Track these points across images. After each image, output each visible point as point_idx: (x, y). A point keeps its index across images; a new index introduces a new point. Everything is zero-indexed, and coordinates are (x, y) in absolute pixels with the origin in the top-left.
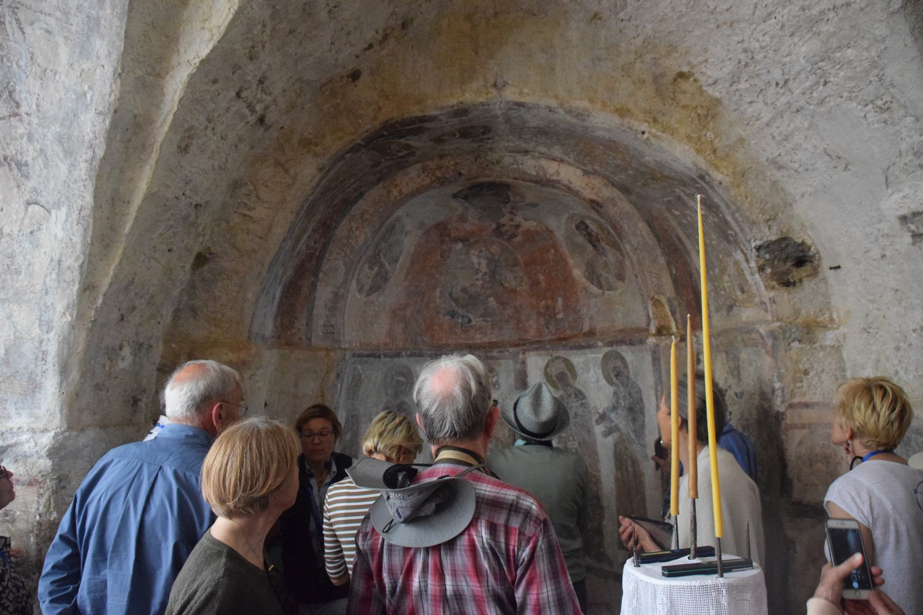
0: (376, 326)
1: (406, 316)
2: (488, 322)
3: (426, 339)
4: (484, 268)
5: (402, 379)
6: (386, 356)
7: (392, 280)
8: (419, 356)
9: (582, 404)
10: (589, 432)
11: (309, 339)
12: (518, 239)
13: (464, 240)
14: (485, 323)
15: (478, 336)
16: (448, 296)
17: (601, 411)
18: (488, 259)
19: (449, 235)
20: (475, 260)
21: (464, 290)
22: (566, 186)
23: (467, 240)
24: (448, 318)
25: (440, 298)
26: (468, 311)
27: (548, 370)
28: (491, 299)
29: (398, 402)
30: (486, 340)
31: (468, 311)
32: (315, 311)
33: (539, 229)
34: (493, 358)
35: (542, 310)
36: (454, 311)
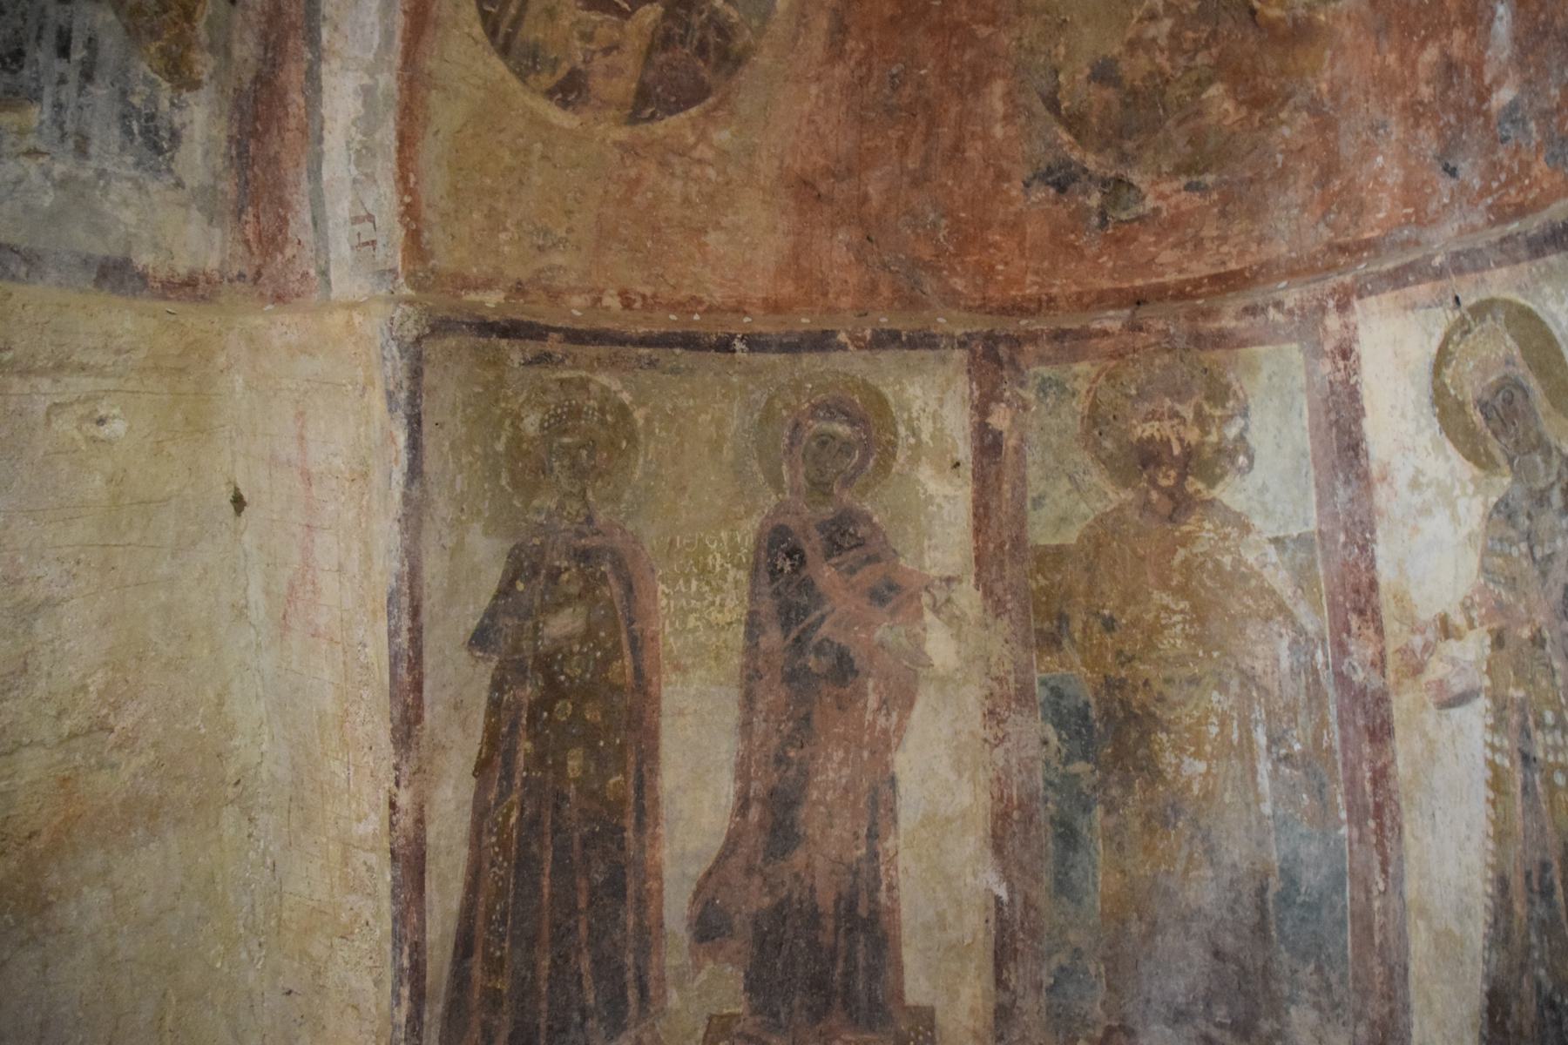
0: (712, 238)
1: (865, 199)
3: (959, 284)
5: (842, 429)
6: (755, 343)
7: (763, 59)
11: (324, 273)
14: (1196, 197)
15: (1167, 256)
16: (1039, 107)
21: (1104, 73)
24: (1042, 193)
25: (1007, 119)
26: (1123, 158)
27: (1448, 372)
28: (1215, 90)
29: (828, 511)
30: (1200, 268)
31: (1123, 158)
32: (326, 174)
34: (1222, 340)
35: (1426, 92)
36: (1068, 164)
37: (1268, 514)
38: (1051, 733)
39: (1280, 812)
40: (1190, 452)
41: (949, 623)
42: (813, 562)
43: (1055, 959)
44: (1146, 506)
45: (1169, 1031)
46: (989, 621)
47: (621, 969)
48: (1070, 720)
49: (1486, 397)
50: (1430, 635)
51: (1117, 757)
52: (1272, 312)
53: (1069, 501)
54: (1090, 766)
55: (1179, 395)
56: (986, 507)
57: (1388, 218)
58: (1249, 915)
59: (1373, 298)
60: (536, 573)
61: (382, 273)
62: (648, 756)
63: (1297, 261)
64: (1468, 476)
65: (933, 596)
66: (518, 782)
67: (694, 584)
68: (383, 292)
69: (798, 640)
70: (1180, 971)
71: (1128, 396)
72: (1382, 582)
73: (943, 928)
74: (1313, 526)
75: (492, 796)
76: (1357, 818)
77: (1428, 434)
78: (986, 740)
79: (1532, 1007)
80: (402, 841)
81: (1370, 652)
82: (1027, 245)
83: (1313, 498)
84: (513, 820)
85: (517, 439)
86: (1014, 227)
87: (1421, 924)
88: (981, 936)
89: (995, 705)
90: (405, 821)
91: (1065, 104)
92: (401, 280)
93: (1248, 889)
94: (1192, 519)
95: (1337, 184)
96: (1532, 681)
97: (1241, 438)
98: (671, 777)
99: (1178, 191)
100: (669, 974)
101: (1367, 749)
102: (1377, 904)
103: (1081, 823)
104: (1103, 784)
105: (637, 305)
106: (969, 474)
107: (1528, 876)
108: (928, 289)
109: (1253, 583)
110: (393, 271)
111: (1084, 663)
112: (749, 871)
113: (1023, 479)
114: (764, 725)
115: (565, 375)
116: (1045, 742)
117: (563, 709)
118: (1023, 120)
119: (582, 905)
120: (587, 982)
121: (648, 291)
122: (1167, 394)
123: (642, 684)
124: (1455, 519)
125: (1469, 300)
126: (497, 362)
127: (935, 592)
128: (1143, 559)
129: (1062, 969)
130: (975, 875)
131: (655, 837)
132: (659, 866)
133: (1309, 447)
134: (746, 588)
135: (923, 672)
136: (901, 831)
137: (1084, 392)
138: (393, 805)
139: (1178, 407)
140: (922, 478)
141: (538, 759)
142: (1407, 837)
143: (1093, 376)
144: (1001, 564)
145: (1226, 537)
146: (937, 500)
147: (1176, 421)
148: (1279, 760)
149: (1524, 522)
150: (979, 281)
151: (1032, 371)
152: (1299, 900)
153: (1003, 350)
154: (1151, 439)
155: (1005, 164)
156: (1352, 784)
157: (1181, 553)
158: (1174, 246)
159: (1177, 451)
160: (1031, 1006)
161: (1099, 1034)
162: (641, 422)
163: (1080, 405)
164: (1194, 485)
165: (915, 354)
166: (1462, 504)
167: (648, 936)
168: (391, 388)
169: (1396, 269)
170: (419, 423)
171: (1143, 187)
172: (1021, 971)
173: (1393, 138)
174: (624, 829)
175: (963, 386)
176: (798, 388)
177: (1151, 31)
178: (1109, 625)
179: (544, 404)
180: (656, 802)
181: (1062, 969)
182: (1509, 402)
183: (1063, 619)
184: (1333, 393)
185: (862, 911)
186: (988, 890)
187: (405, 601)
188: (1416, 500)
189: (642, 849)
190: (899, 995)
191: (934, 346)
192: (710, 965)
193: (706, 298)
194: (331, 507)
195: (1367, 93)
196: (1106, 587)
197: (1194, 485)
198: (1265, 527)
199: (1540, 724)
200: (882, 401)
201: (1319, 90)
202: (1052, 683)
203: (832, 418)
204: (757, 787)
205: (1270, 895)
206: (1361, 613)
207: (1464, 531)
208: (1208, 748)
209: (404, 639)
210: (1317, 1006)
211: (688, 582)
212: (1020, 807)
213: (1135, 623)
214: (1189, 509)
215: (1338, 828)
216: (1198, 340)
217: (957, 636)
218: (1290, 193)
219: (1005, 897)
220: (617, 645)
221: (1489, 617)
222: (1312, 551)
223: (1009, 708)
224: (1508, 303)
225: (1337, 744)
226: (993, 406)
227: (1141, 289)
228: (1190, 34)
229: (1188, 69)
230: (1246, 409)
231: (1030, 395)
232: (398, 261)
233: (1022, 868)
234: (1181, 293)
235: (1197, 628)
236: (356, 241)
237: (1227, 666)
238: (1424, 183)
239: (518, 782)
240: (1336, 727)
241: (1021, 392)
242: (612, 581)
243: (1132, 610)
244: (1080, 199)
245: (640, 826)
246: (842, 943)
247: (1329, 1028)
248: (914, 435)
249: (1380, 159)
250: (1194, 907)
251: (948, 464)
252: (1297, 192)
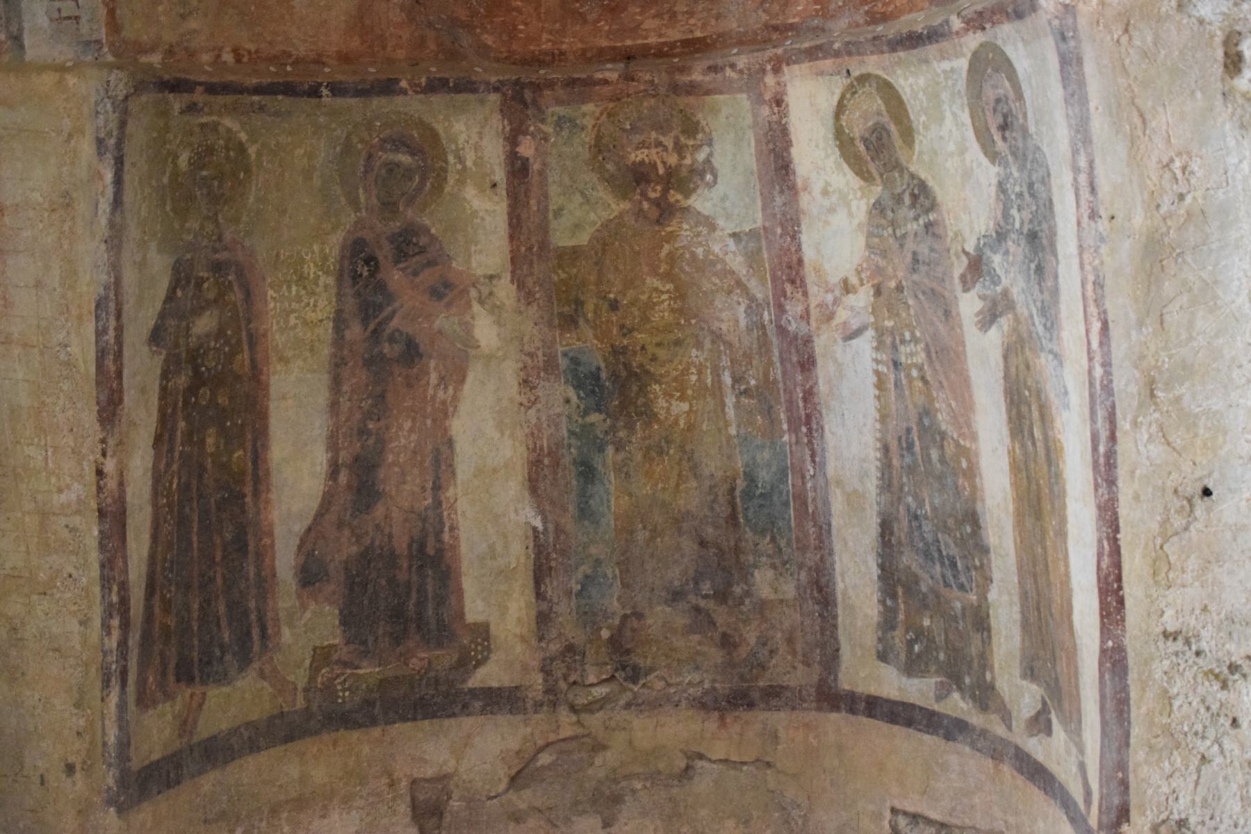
3: (489, 40)
5: (404, 158)
6: (337, 90)
8: (458, 89)
9: (928, 226)
10: (947, 313)
15: (650, 24)
17: (970, 248)
27: (844, 118)
29: (396, 226)
30: (674, 34)
34: (692, 89)
37: (728, 217)
38: (571, 393)
39: (742, 431)
40: (671, 172)
41: (491, 312)
42: (386, 269)
43: (582, 568)
44: (640, 213)
45: (668, 609)
46: (522, 309)
47: (246, 613)
48: (588, 384)
49: (867, 135)
50: (837, 293)
51: (623, 406)
52: (728, 72)
53: (581, 211)
54: (603, 416)
55: (662, 128)
56: (518, 218)
57: (805, 10)
58: (723, 510)
59: (796, 67)
60: (188, 282)
61: (88, 43)
62: (261, 434)
63: (746, 33)
64: (857, 187)
65: (480, 292)
66: (177, 455)
67: (294, 289)
68: (89, 58)
69: (375, 331)
70: (676, 562)
71: (624, 130)
72: (806, 259)
73: (493, 558)
74: (759, 223)
75: (162, 466)
76: (794, 429)
77: (832, 159)
78: (521, 404)
79: (905, 523)
80: (109, 500)
81: (799, 309)
83: (759, 203)
84: (174, 486)
85: (175, 174)
87: (838, 491)
88: (522, 560)
89: (528, 375)
90: (111, 484)
92: (106, 49)
93: (722, 490)
94: (674, 222)
96: (898, 315)
97: (708, 161)
98: (278, 451)
100: (282, 614)
101: (799, 377)
102: (809, 485)
103: (597, 462)
104: (613, 428)
105: (245, 59)
106: (504, 193)
107: (900, 439)
108: (465, 44)
109: (719, 267)
110: (98, 42)
111: (596, 337)
112: (340, 525)
113: (546, 196)
114: (348, 403)
115: (204, 120)
116: (568, 401)
117: (205, 392)
119: (218, 559)
120: (224, 622)
121: (252, 47)
122: (653, 128)
123: (257, 376)
124: (850, 214)
125: (856, 73)
126: (165, 113)
127: (482, 288)
128: (638, 253)
129: (586, 577)
130: (516, 511)
131: (267, 502)
132: (271, 525)
133: (755, 168)
134: (334, 291)
135: (472, 352)
136: (459, 482)
137: (590, 126)
138: (100, 473)
139: (662, 138)
140: (468, 196)
141: (189, 435)
142: (827, 434)
143: (597, 115)
144: (531, 264)
145: (699, 234)
146: (481, 214)
147: (659, 149)
148: (741, 393)
149: (889, 213)
150: (505, 37)
151: (551, 110)
152: (758, 492)
153: (528, 95)
154: (642, 163)
156: (791, 403)
157: (667, 248)
158: (654, 17)
159: (661, 171)
160: (564, 610)
161: (617, 622)
162: (253, 157)
163: (588, 137)
164: (674, 196)
165: (460, 97)
166: (854, 203)
167: (265, 584)
168: (102, 135)
169: (811, 48)
170: (122, 163)
172: (555, 583)
174: (244, 496)
175: (497, 123)
176: (369, 126)
178: (614, 306)
179: (191, 144)
180: (268, 473)
181: (586, 577)
182: (879, 139)
183: (579, 303)
184: (771, 129)
185: (430, 551)
186: (527, 523)
187: (112, 305)
188: (826, 203)
189: (258, 513)
190: (461, 615)
191: (474, 91)
192: (312, 606)
193: (294, 52)
194: (27, 234)
196: (611, 277)
197: (674, 196)
198: (726, 226)
199: (903, 342)
200: (435, 135)
202: (571, 354)
203: (397, 150)
204: (344, 456)
205: (737, 493)
206: (793, 282)
207: (856, 222)
208: (690, 392)
209: (110, 336)
210: (774, 566)
211: (289, 288)
212: (549, 454)
213: (632, 303)
214: (672, 214)
215: (782, 437)
216: (675, 89)
217: (498, 323)
219: (540, 527)
220: (239, 341)
221: (870, 278)
222: (759, 240)
223: (539, 377)
224: (878, 77)
225: (779, 377)
226: (521, 138)
230: (711, 140)
231: (549, 129)
232: (102, 34)
233: (552, 503)
234: (661, 52)
235: (679, 303)
236: (56, 15)
237: (703, 329)
239: (177, 455)
240: (778, 364)
241: (543, 127)
242: (236, 288)
243: (631, 293)
245: (256, 494)
246: (415, 578)
247: (782, 580)
248: (460, 162)
250: (683, 510)
251: (488, 185)
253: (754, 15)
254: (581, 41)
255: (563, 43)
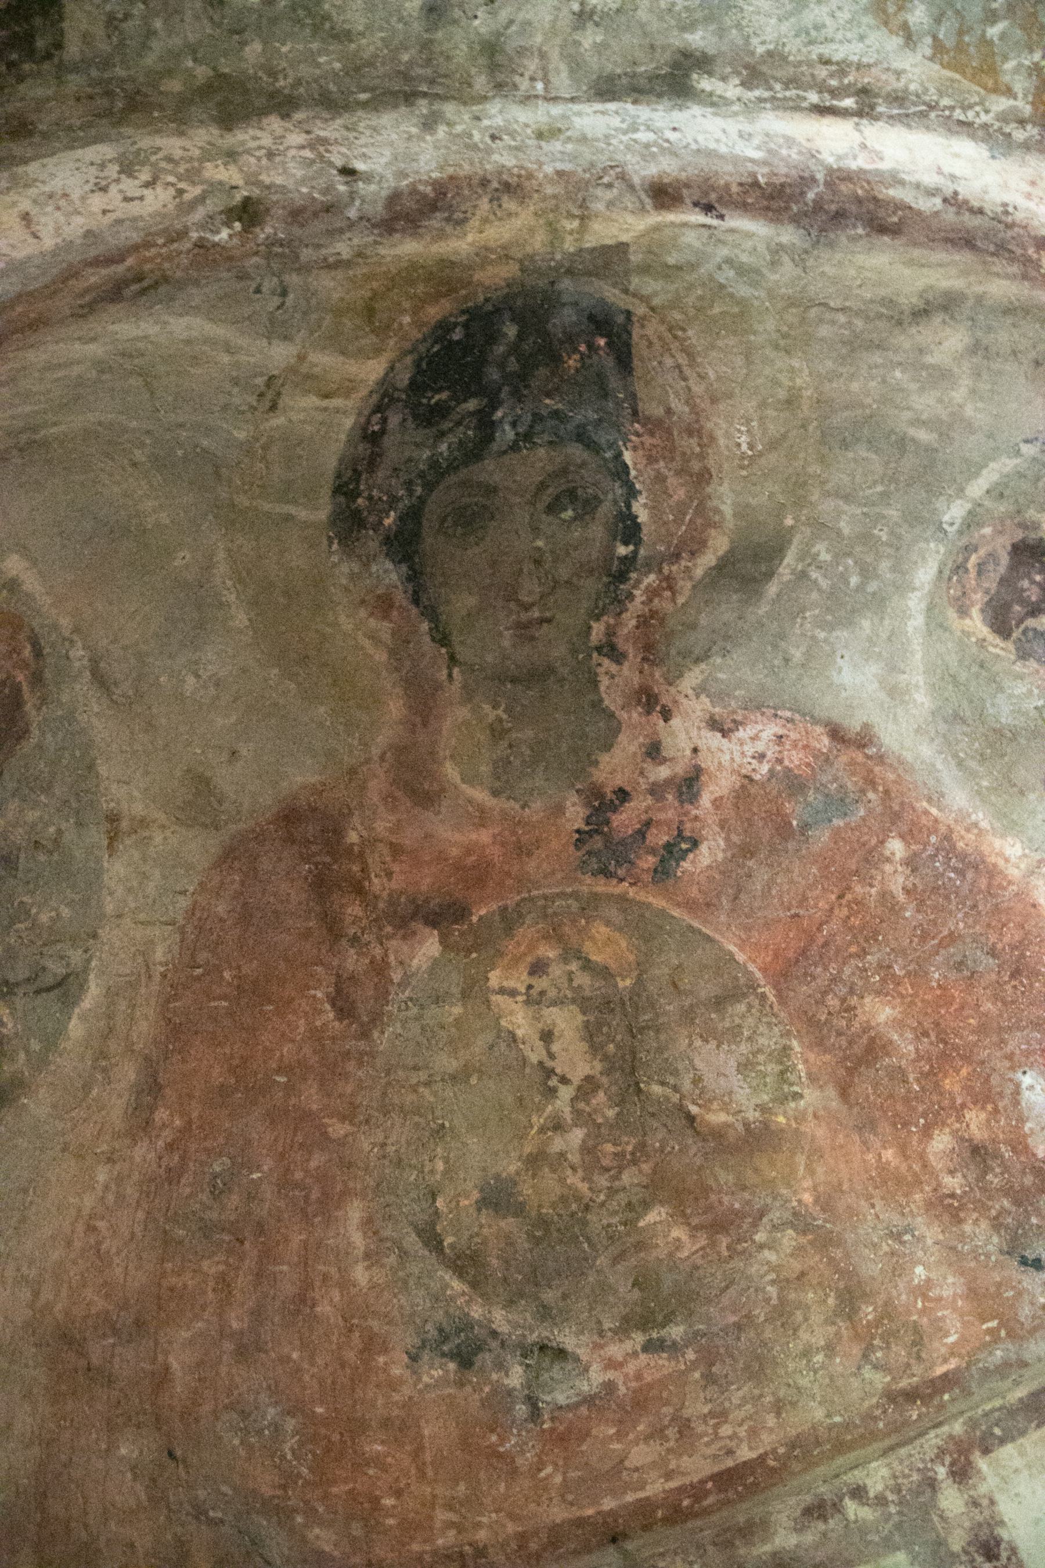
1: (162, 1378)
2: (674, 1349)
4: (575, 1061)
12: (710, 853)
13: (444, 914)
14: (663, 1364)
15: (640, 1455)
16: (412, 1241)
18: (583, 1003)
19: (359, 890)
20: (519, 1020)
21: (498, 1198)
22: (932, 192)
23: (459, 912)
24: (436, 1371)
25: (371, 1257)
26: (545, 1313)
28: (655, 1215)
30: (697, 1467)
33: (794, 759)
35: (953, 1183)
36: (466, 1325)
52: (851, 1507)
57: (963, 1339)
63: (847, 1426)
82: (428, 1457)
86: (402, 1428)
91: (449, 1240)
95: (868, 1312)
99: (635, 1354)
118: (392, 1260)
150: (357, 1529)
155: (374, 1324)
158: (648, 1438)
171: (583, 1353)
173: (929, 1242)
177: (558, 1144)
195: (869, 1197)
201: (800, 1201)
218: (804, 1335)
227: (611, 1513)
228: (609, 1148)
229: (612, 1192)
234: (676, 1512)
238: (999, 1285)
244: (494, 1376)
249: (919, 1270)
252: (815, 1333)
253: (855, 1383)
254: (512, 1517)
255: (478, 1525)
